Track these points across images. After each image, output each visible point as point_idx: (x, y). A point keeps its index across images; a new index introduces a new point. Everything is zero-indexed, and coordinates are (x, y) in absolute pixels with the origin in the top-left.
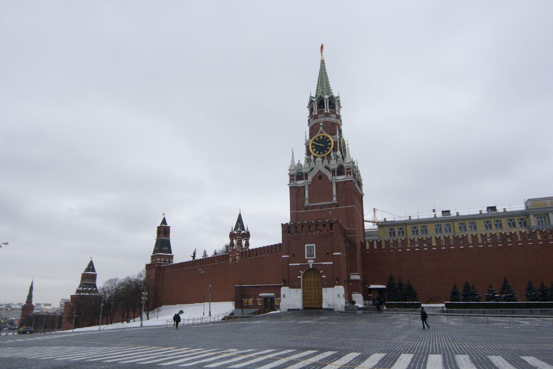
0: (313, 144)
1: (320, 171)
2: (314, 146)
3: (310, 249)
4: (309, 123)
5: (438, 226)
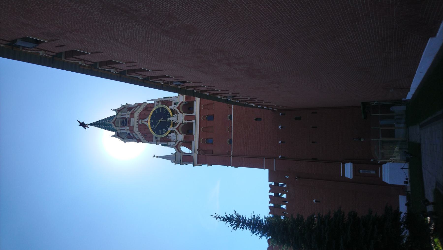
0: (157, 133)
2: (160, 131)
4: (139, 141)
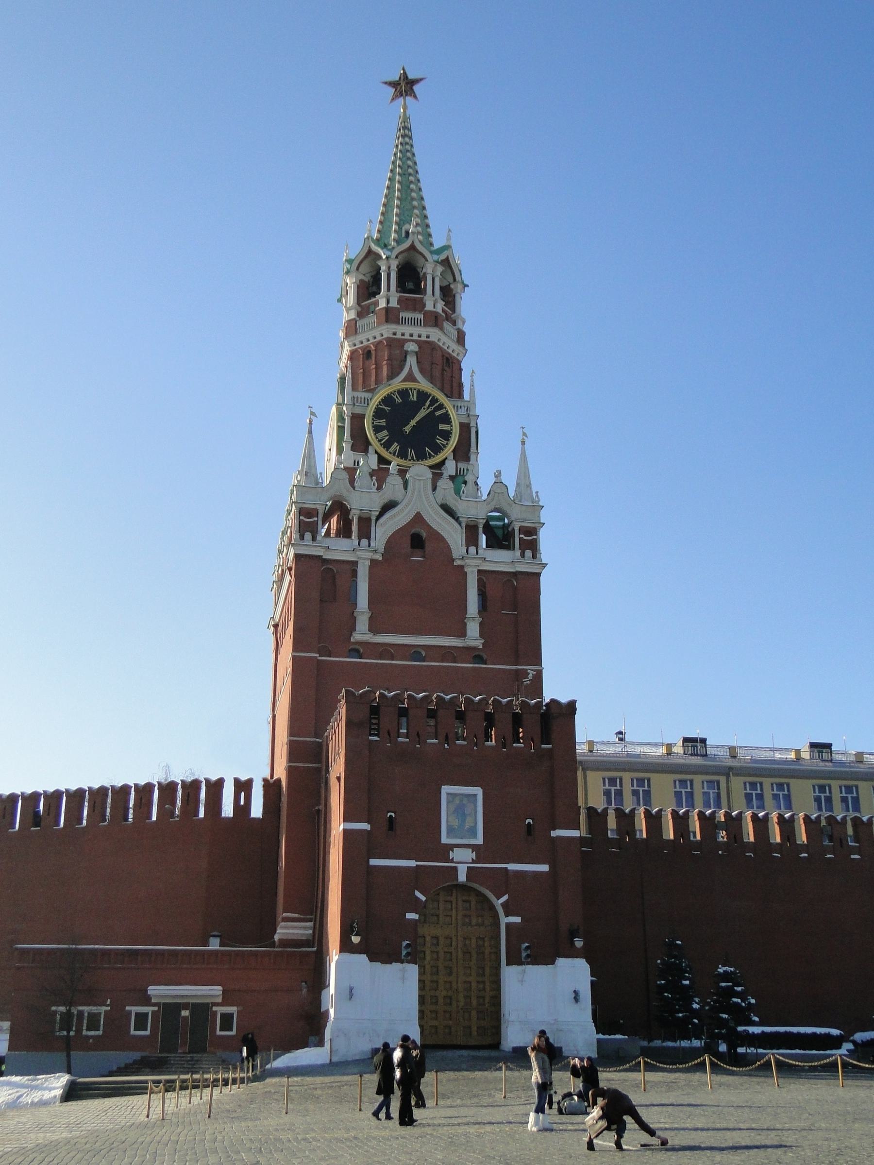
0: (378, 413)
1: (418, 518)
2: (383, 422)
3: (461, 808)
5: (683, 783)
